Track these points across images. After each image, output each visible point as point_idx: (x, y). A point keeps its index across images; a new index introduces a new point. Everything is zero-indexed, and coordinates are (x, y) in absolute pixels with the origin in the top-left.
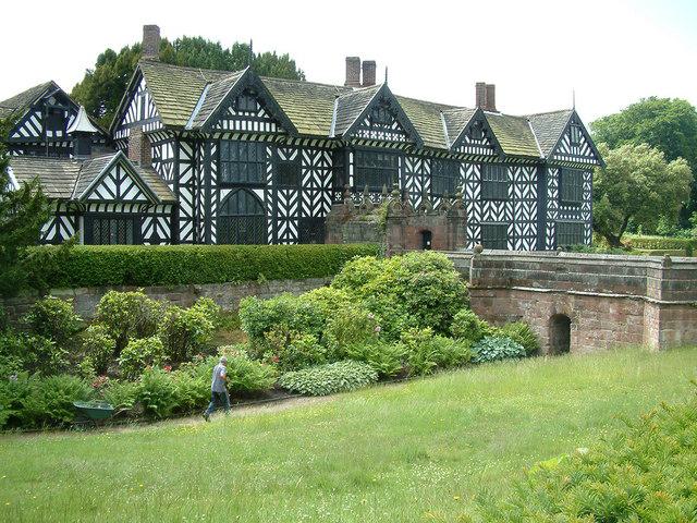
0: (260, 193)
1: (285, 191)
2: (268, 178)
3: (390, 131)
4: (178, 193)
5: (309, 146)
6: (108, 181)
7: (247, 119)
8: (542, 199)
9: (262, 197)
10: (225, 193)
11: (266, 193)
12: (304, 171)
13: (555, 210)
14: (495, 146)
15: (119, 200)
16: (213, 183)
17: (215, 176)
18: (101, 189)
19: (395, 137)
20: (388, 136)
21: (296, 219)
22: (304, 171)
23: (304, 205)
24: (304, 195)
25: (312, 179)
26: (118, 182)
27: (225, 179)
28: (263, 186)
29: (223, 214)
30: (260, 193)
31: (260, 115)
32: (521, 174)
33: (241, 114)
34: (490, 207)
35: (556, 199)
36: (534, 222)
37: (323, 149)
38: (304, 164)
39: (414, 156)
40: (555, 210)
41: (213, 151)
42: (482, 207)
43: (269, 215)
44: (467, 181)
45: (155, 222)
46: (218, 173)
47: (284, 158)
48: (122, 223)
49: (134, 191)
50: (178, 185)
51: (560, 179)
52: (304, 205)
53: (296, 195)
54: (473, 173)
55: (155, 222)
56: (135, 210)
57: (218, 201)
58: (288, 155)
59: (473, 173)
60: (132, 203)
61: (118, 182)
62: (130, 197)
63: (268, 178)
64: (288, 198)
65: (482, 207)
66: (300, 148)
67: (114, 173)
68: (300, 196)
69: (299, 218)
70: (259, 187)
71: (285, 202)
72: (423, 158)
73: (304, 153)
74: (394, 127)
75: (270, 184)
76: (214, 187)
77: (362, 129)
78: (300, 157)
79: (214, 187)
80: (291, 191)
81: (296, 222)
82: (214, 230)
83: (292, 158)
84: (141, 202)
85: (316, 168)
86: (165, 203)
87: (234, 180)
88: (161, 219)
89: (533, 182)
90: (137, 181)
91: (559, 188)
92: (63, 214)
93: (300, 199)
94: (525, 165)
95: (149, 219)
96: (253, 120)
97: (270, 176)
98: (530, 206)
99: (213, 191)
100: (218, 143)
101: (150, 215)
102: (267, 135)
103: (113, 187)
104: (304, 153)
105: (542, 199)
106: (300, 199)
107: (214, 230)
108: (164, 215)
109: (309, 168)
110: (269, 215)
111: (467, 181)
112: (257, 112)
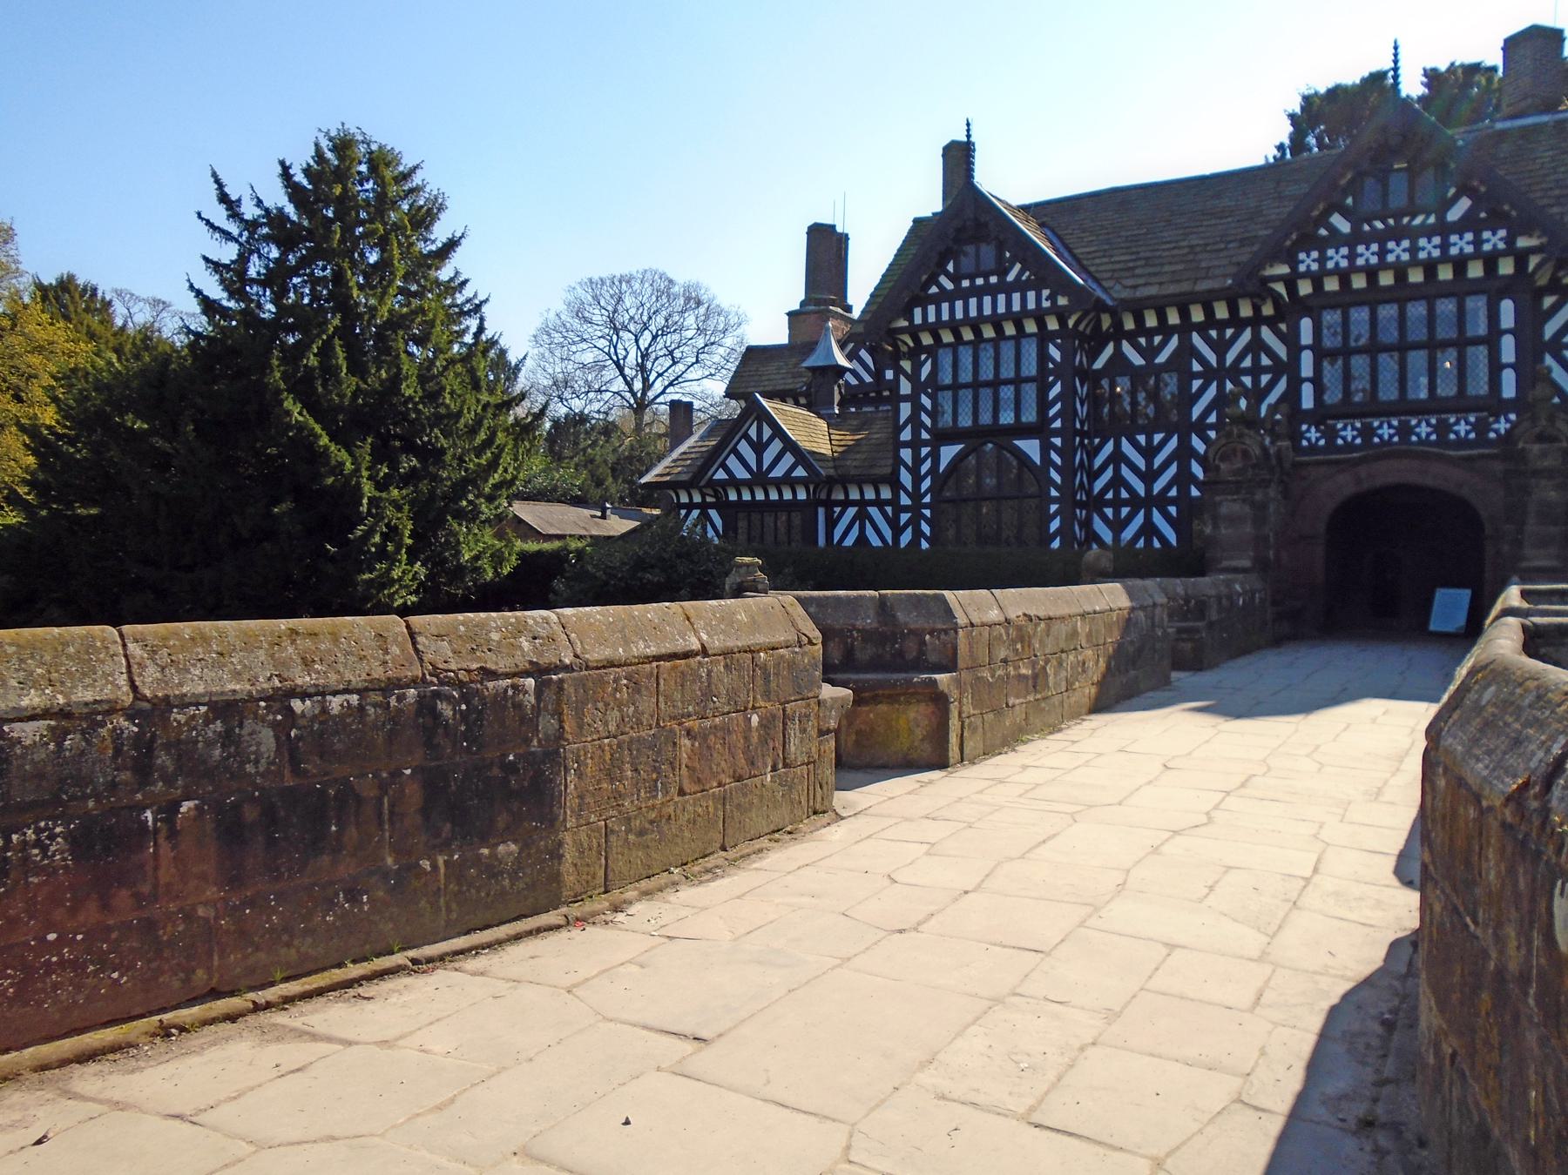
0: (1031, 447)
1: (1142, 439)
2: (1052, 412)
6: (744, 448)
7: (979, 293)
10: (948, 453)
11: (1046, 448)
12: (1196, 384)
15: (760, 478)
16: (925, 435)
17: (927, 421)
18: (732, 462)
19: (1461, 244)
22: (1196, 384)
26: (759, 448)
27: (946, 420)
28: (1039, 430)
30: (1031, 447)
31: (1011, 277)
38: (1196, 367)
41: (926, 371)
45: (862, 516)
46: (933, 415)
47: (1138, 360)
48: (755, 517)
49: (789, 459)
53: (1173, 443)
55: (862, 516)
56: (802, 495)
57: (931, 472)
58: (1149, 353)
60: (788, 480)
61: (759, 448)
62: (778, 472)
63: (1052, 412)
64: (1149, 452)
67: (753, 432)
68: (1185, 445)
69: (1183, 500)
70: (1026, 431)
71: (1141, 463)
73: (1196, 339)
74: (1454, 215)
75: (1057, 424)
76: (925, 443)
78: (1187, 351)
79: (925, 443)
80: (1158, 438)
81: (1173, 510)
82: (926, 528)
83: (1161, 359)
84: (804, 482)
87: (966, 421)
92: (712, 506)
93: (1184, 453)
95: (852, 511)
96: (993, 291)
97: (1059, 406)
99: (925, 451)
100: (932, 351)
104: (1196, 339)
107: (926, 528)
110: (1054, 493)
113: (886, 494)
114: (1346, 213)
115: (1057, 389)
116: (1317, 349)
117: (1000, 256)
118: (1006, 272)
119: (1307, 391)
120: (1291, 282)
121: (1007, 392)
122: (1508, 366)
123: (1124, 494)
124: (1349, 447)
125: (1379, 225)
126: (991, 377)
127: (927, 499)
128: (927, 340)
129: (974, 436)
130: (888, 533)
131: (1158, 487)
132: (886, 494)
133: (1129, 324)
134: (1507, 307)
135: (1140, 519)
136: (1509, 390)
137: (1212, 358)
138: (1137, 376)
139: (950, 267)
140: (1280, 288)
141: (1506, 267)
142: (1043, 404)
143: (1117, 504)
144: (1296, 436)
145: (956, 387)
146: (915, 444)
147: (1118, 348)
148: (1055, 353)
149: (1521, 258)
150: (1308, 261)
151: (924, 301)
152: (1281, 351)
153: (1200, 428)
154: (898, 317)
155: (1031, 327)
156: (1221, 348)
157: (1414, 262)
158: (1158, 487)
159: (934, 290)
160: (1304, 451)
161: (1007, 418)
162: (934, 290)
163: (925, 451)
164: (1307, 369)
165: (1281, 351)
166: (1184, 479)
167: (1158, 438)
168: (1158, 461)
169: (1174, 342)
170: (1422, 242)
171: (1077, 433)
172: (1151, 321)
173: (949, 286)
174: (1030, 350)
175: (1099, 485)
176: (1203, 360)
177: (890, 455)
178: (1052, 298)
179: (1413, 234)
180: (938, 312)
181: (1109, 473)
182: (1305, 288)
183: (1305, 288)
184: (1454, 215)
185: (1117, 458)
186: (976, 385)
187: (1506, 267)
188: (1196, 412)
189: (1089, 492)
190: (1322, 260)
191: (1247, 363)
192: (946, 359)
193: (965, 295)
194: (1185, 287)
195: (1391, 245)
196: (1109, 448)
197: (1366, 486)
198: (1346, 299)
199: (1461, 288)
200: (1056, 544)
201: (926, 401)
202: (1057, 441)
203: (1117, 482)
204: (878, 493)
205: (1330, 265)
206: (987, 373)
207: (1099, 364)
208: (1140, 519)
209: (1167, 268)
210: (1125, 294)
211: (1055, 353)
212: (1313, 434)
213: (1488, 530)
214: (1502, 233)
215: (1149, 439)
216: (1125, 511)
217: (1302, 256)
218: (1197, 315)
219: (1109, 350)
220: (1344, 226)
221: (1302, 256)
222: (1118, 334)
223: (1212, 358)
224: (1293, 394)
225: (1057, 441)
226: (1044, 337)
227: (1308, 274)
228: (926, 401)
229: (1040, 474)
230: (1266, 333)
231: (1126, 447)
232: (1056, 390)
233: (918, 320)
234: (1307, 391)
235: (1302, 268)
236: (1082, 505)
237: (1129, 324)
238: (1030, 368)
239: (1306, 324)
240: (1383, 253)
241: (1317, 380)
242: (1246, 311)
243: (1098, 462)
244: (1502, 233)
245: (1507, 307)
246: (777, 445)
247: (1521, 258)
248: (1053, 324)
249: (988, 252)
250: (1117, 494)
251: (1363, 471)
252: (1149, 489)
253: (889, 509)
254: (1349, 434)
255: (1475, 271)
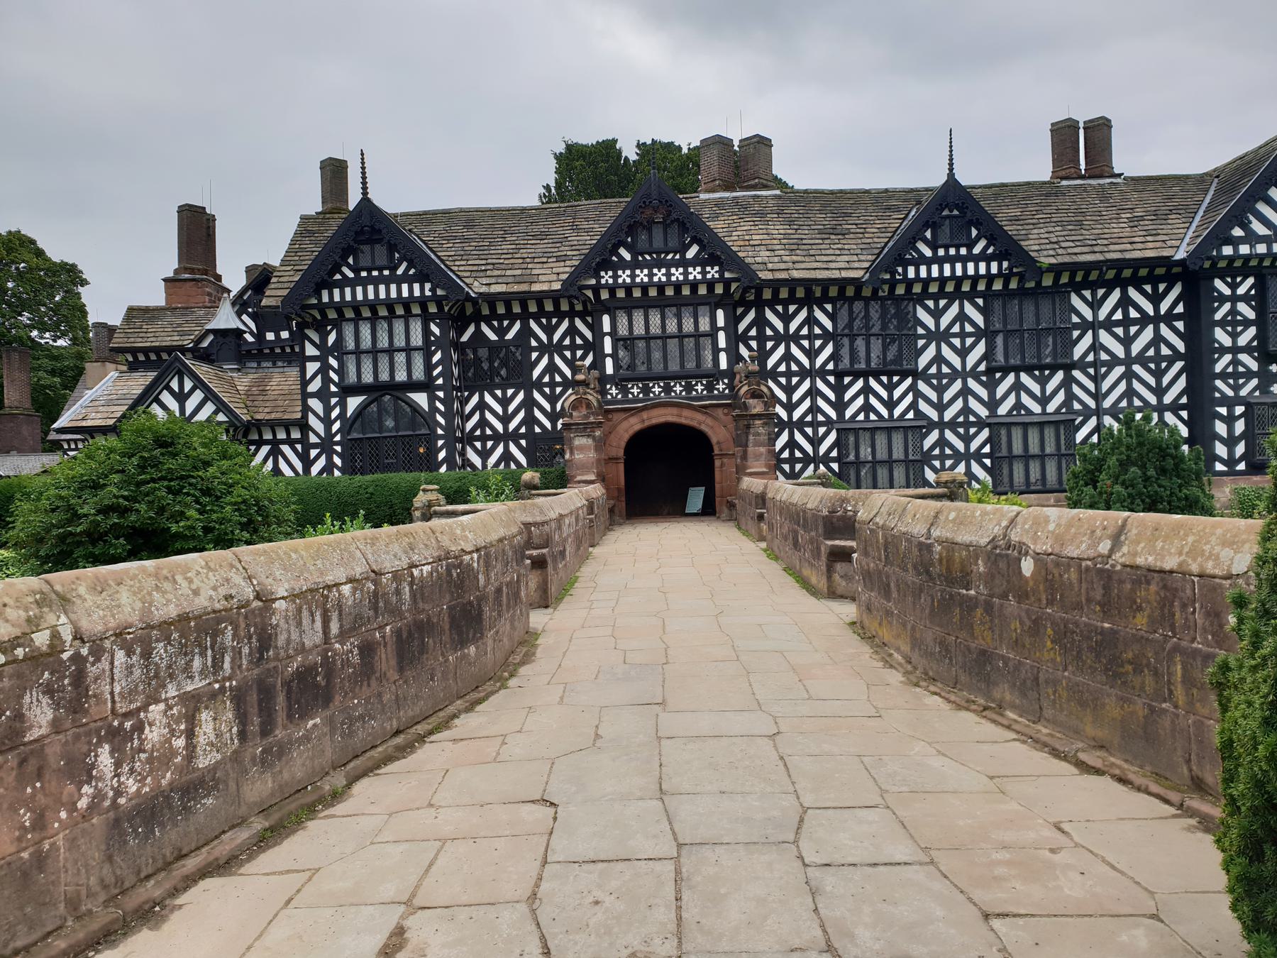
0: (421, 399)
1: (499, 393)
2: (435, 373)
3: (685, 263)
4: (306, 409)
5: (541, 312)
6: (166, 397)
7: (376, 282)
8: (1198, 358)
9: (425, 406)
10: (353, 403)
11: (432, 398)
12: (534, 355)
13: (1249, 375)
14: (1006, 248)
16: (333, 388)
19: (695, 273)
20: (677, 274)
21: (523, 436)
22: (534, 355)
23: (537, 414)
24: (537, 395)
25: (552, 368)
26: (181, 398)
27: (352, 378)
28: (426, 386)
29: (355, 435)
30: (421, 399)
31: (400, 272)
32: (1125, 302)
33: (364, 274)
34: (1018, 387)
35: (1247, 349)
36: (1175, 408)
37: (572, 314)
38: (534, 343)
39: (785, 303)
40: (1249, 375)
41: (332, 338)
42: (991, 386)
43: (440, 432)
44: (941, 336)
45: (275, 453)
46: (341, 372)
47: (493, 337)
49: (209, 408)
50: (305, 396)
51: (1260, 300)
52: (537, 414)
53: (521, 396)
54: (962, 317)
55: (275, 453)
58: (501, 332)
59: (962, 317)
61: (181, 398)
62: (202, 416)
63: (435, 373)
64: (505, 402)
65: (991, 386)
66: (525, 316)
67: (175, 385)
69: (530, 435)
72: (809, 301)
73: (533, 324)
74: (690, 254)
75: (440, 381)
76: (334, 395)
77: (614, 268)
78: (526, 333)
79: (334, 395)
81: (523, 442)
82: (337, 461)
83: (510, 336)
85: (559, 348)
86: (287, 425)
87: (368, 378)
88: (286, 449)
89: (1169, 318)
90: (210, 396)
91: (1261, 322)
93: (529, 403)
94: (1138, 284)
95: (265, 449)
97: (440, 368)
98: (1158, 374)
99: (334, 401)
100: (337, 325)
101: (267, 442)
102: (423, 302)
103: (173, 405)
104: (533, 324)
105: (1198, 358)
106: (529, 403)
107: (337, 461)
108: (291, 443)
109: (543, 349)
110: (440, 432)
111: (941, 336)
112: (393, 269)
113: (296, 435)
114: (628, 249)
115: (438, 356)
116: (613, 333)
117: (391, 257)
118: (396, 268)
119: (609, 363)
120: (596, 289)
121: (400, 358)
122: (722, 350)
123: (489, 432)
124: (636, 400)
125: (648, 257)
126: (387, 345)
127: (338, 438)
128: (332, 315)
129: (375, 390)
130: (299, 465)
131: (512, 426)
132: (296, 435)
133: (486, 311)
134: (720, 314)
135: (500, 450)
136: (723, 365)
137: (544, 337)
138: (493, 348)
139: (351, 261)
140: (589, 293)
141: (719, 289)
142: (429, 367)
143: (484, 438)
144: (603, 392)
145: (358, 352)
146: (323, 395)
147: (478, 328)
148: (436, 330)
149: (727, 284)
150: (607, 278)
151: (330, 286)
152: (589, 335)
153: (539, 385)
154: (310, 296)
155: (416, 310)
156: (550, 331)
157: (669, 282)
158: (512, 426)
159: (338, 277)
160: (609, 403)
161: (401, 376)
162: (338, 277)
163: (334, 401)
164: (608, 348)
165: (589, 335)
166: (530, 421)
167: (510, 392)
168: (511, 408)
169: (517, 326)
170: (673, 270)
171: (455, 388)
172: (501, 310)
173: (351, 275)
174: (416, 328)
175: (470, 425)
176: (538, 339)
177: (300, 403)
178: (433, 290)
179: (669, 265)
180: (342, 295)
181: (476, 417)
182: (605, 295)
183: (605, 295)
184: (690, 254)
185: (482, 406)
186: (374, 352)
187: (719, 289)
188: (536, 373)
189: (463, 431)
190: (615, 277)
191: (567, 342)
192: (348, 331)
193: (364, 283)
194: (524, 287)
195: (655, 271)
196: (475, 399)
197: (647, 424)
198: (629, 306)
199: (695, 303)
200: (443, 469)
201: (333, 362)
202: (441, 394)
203: (483, 423)
204: (288, 434)
205: (620, 281)
206: (383, 342)
207: (465, 338)
208: (500, 450)
209: (509, 272)
210: (484, 289)
211: (436, 330)
212: (614, 391)
213: (716, 452)
214: (717, 268)
215: (504, 393)
216: (490, 444)
217: (603, 273)
218: (533, 308)
219: (471, 329)
220: (627, 256)
221: (603, 273)
222: (477, 318)
223: (544, 337)
224: (598, 364)
225: (441, 394)
226: (426, 318)
227: (607, 286)
228: (333, 362)
229: (428, 419)
230: (579, 324)
231: (488, 399)
232: (438, 356)
233: (325, 299)
234: (609, 363)
235: (603, 281)
236: (461, 440)
237: (486, 311)
238: (417, 340)
239: (606, 320)
240: (651, 275)
241: (614, 356)
242: (565, 307)
243: (468, 408)
244: (717, 268)
245: (720, 314)
246: (198, 396)
247: (727, 284)
248: (433, 309)
249: (381, 252)
250: (483, 431)
251: (645, 415)
252: (506, 428)
253: (299, 447)
254: (635, 391)
255: (702, 290)
